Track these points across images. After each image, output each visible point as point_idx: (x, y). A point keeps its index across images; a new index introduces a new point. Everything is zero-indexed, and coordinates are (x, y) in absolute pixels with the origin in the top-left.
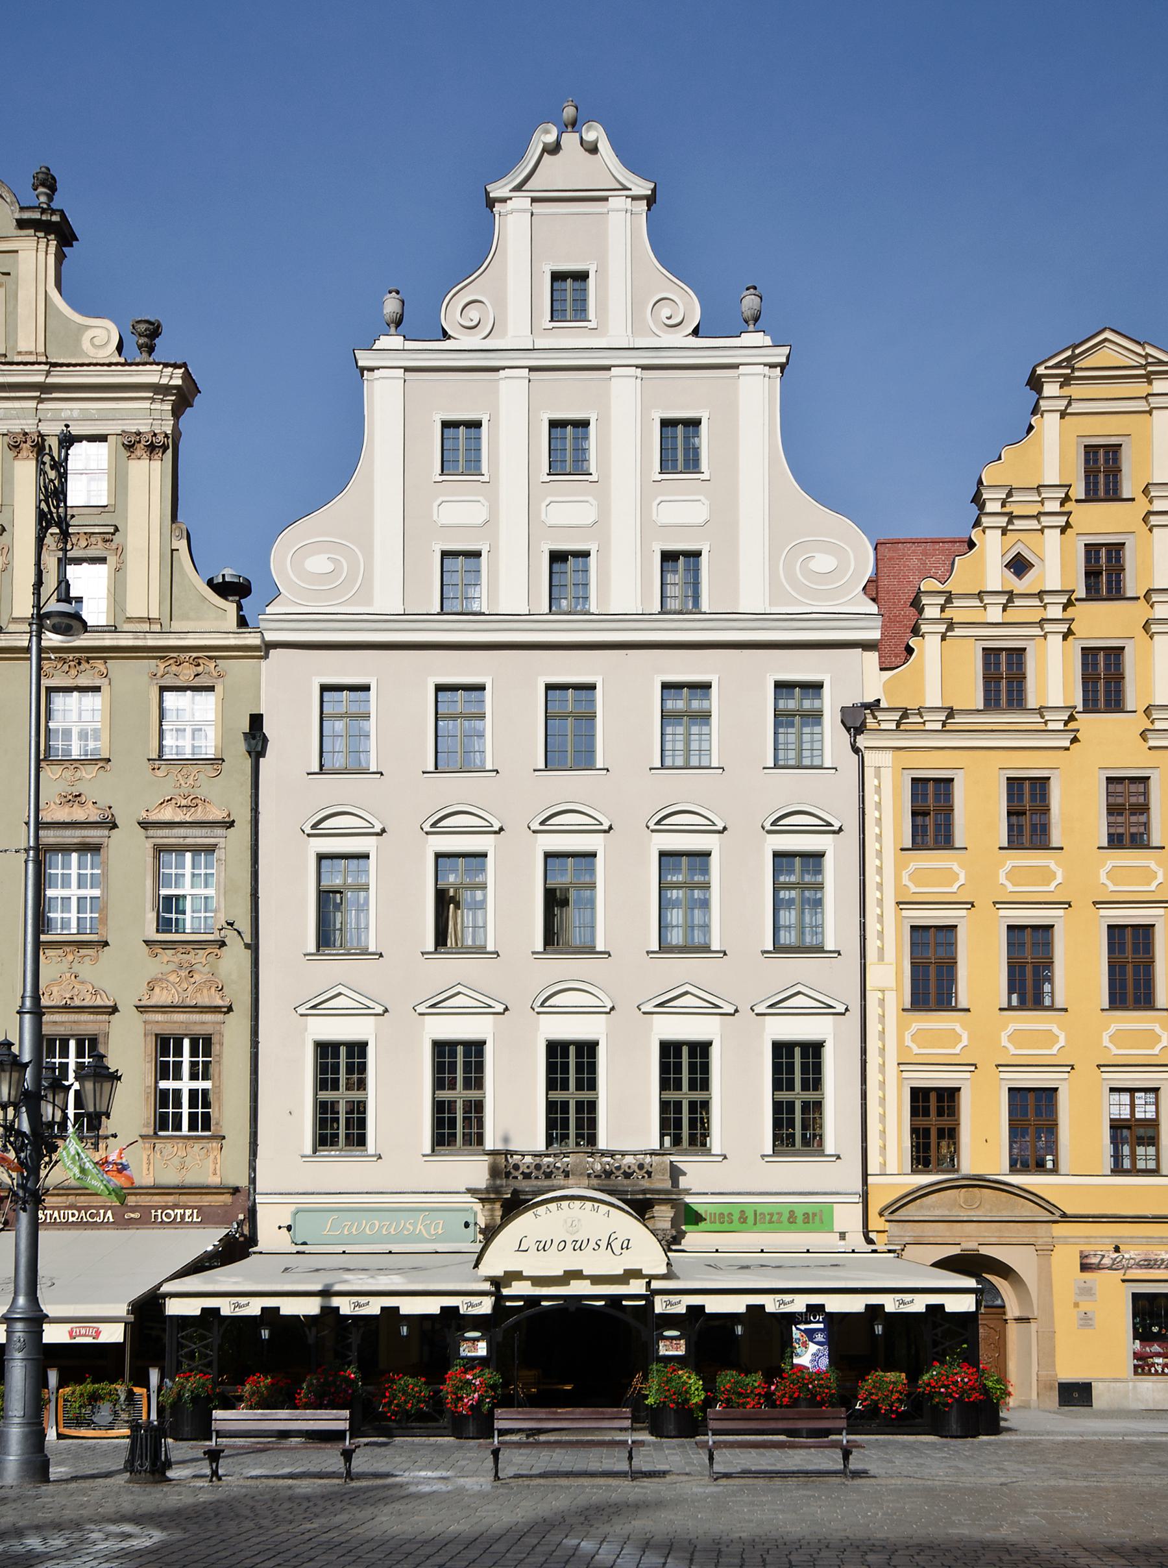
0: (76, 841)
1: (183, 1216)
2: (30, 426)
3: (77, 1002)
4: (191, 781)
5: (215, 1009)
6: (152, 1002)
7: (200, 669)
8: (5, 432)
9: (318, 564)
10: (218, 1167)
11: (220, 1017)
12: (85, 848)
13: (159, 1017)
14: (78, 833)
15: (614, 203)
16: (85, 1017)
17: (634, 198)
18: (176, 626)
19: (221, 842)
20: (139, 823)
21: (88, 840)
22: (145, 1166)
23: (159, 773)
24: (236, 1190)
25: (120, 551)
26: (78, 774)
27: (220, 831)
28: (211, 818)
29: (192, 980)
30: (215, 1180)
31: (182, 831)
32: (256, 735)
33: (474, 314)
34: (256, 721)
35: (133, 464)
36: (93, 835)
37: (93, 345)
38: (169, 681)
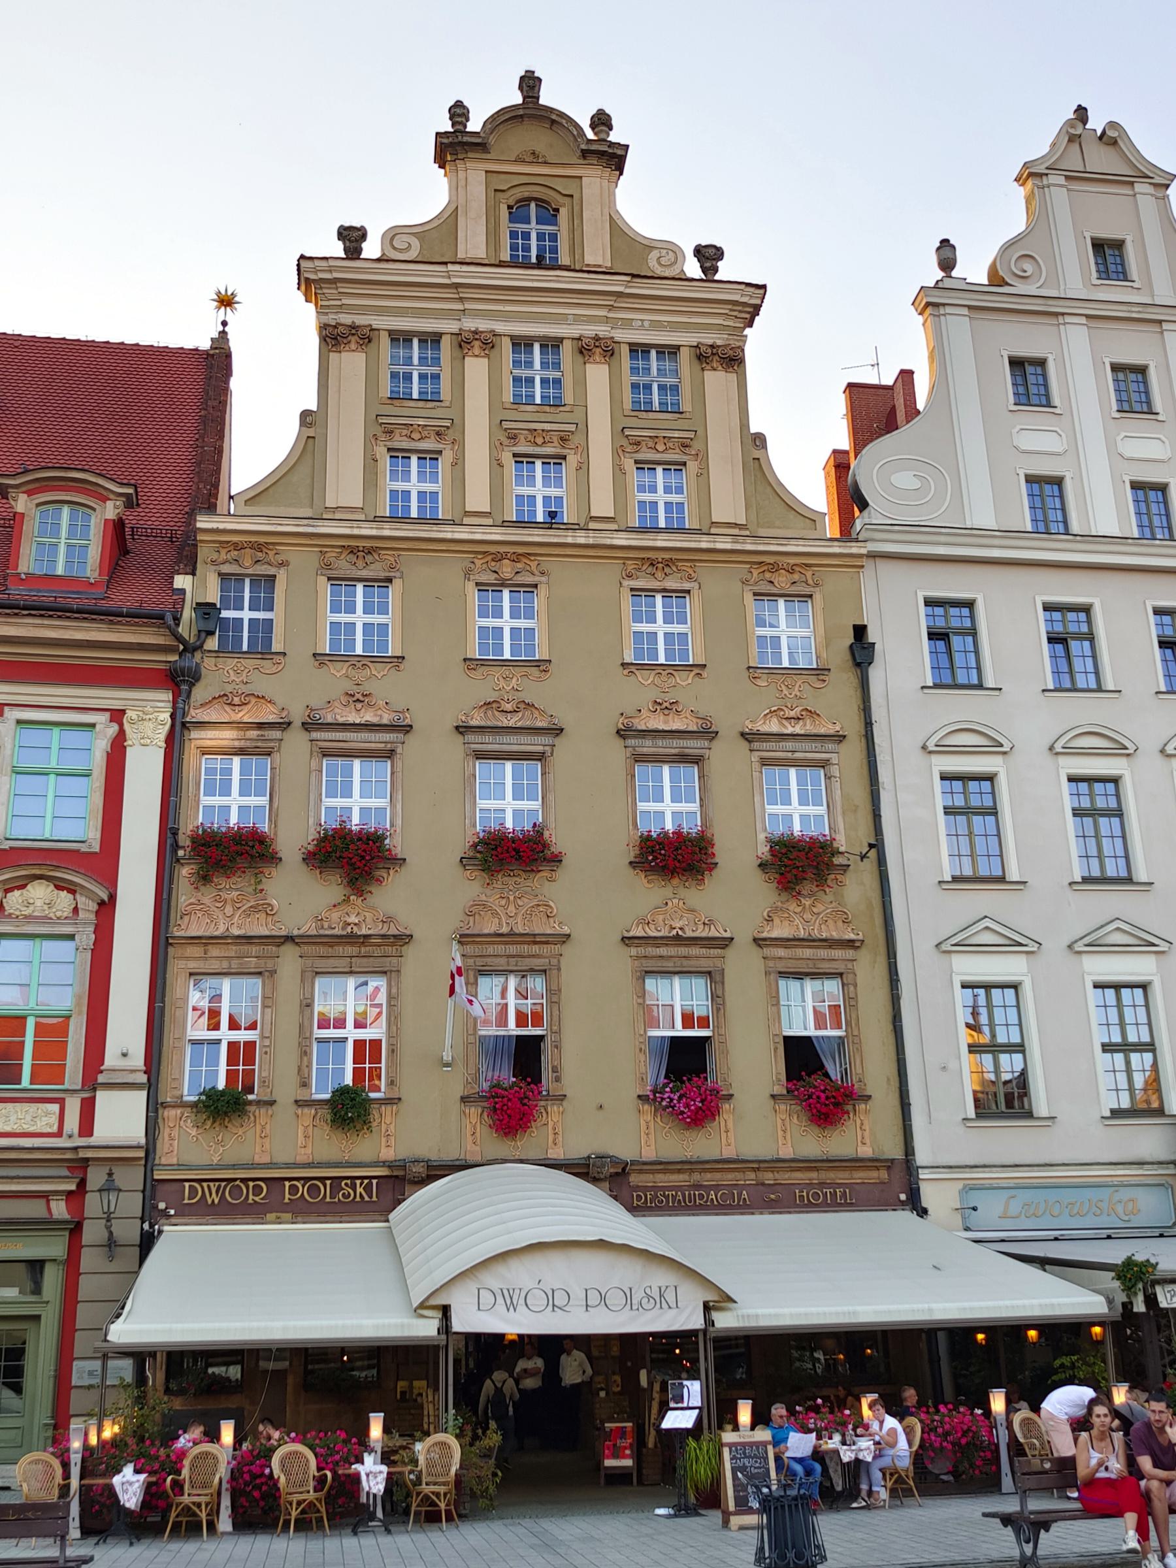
0: (673, 751)
1: (834, 1195)
2: (602, 330)
3: (689, 933)
4: (796, 692)
5: (850, 944)
6: (774, 934)
7: (796, 577)
8: (577, 336)
9: (905, 480)
10: (867, 1134)
11: (850, 954)
12: (683, 758)
13: (781, 952)
14: (676, 743)
15: (1138, 188)
16: (695, 951)
17: (1155, 185)
18: (762, 532)
19: (834, 758)
20: (743, 734)
21: (687, 751)
22: (780, 1133)
23: (759, 682)
24: (889, 1164)
25: (702, 457)
26: (672, 681)
27: (830, 746)
28: (822, 731)
29: (815, 910)
30: (866, 1151)
31: (790, 745)
32: (861, 648)
33: (1029, 267)
34: (860, 631)
35: (709, 375)
36: (693, 746)
37: (660, 264)
38: (764, 587)
